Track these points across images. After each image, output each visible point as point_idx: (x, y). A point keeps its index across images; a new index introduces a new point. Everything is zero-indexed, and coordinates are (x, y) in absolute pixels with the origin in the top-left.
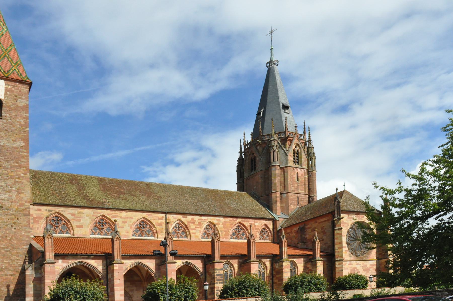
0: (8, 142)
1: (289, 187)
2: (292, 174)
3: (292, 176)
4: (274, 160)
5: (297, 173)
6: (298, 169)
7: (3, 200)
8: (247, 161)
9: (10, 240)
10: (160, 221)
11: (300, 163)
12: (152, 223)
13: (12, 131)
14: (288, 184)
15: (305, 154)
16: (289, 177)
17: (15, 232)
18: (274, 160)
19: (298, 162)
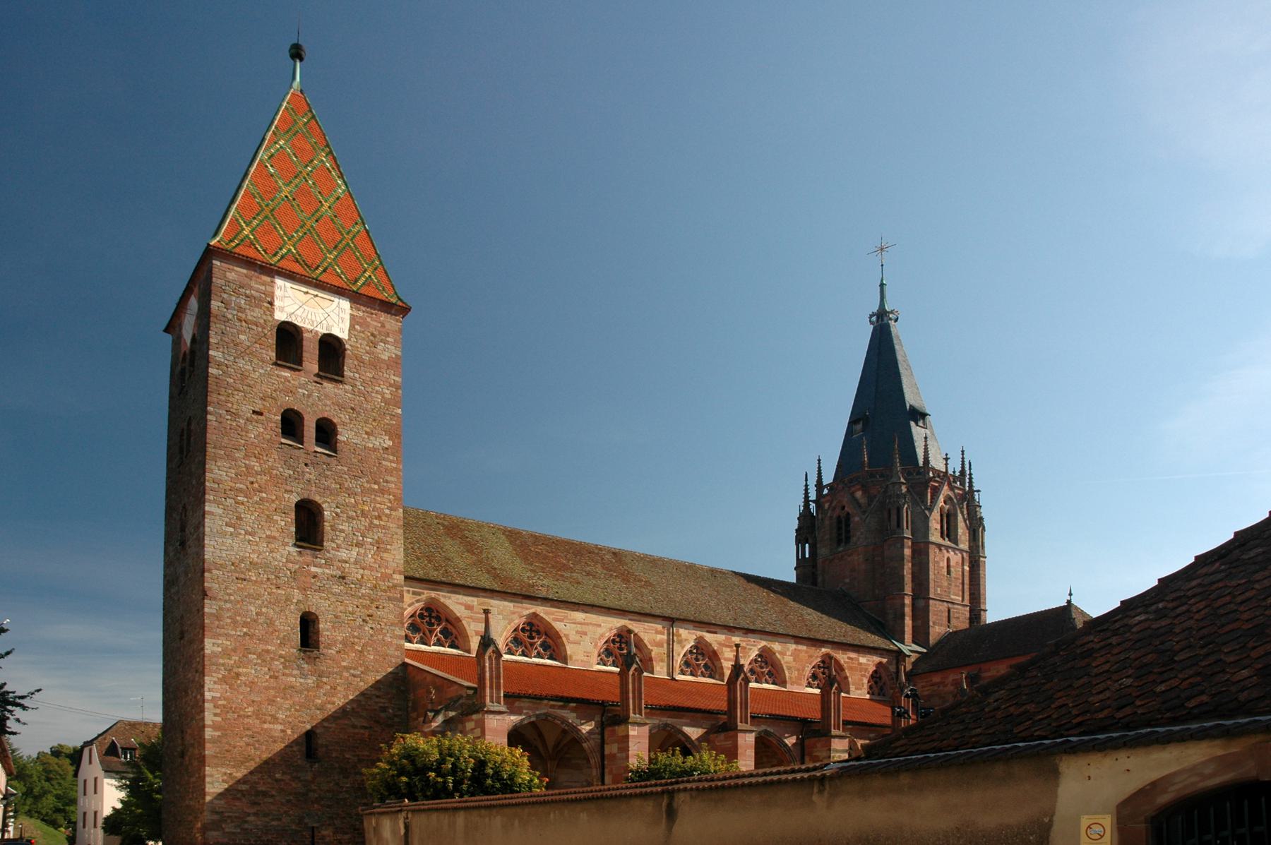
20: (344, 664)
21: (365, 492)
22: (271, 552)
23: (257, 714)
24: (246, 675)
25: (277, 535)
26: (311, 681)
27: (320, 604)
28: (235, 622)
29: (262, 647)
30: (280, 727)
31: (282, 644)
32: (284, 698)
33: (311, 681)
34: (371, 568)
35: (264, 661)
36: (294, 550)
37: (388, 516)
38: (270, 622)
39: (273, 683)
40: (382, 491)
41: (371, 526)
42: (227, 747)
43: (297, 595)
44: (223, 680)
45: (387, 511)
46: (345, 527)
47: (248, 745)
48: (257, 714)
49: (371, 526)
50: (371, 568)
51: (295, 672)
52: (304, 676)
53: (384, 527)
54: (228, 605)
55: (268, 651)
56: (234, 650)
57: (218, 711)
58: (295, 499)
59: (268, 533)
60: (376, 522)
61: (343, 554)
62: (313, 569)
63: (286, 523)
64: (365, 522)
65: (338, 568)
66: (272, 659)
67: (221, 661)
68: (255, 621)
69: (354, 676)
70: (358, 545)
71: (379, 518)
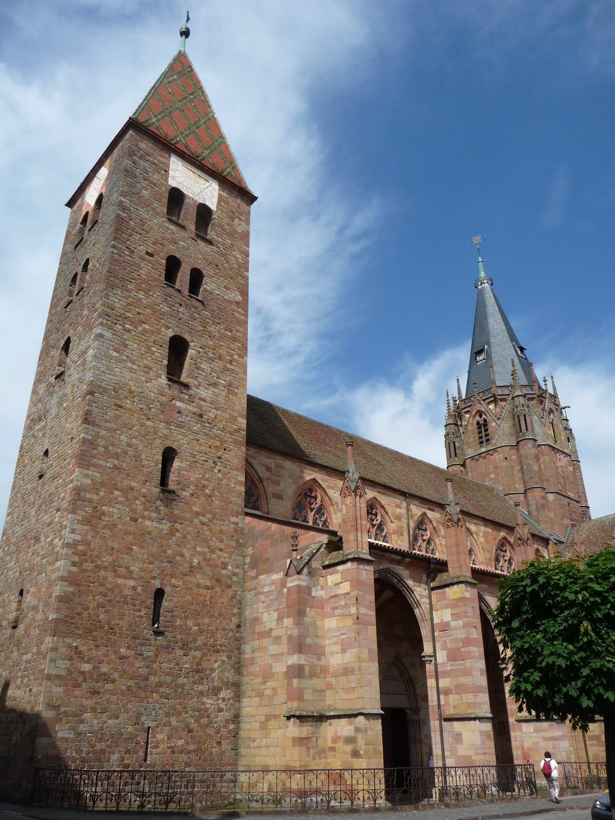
4: (527, 430)
8: (470, 428)
9: (210, 496)
10: (398, 510)
12: (387, 513)
17: (220, 480)
18: (527, 430)
20: (195, 509)
21: (222, 337)
22: (147, 382)
24: (111, 515)
25: (151, 365)
27: (180, 441)
29: (126, 483)
30: (131, 583)
33: (165, 527)
35: (128, 500)
36: (163, 380)
38: (137, 458)
41: (225, 369)
42: (79, 610)
44: (87, 521)
47: (100, 606)
48: (114, 567)
49: (225, 369)
51: (154, 515)
52: (159, 521)
53: (232, 371)
54: (103, 432)
55: (132, 488)
56: (103, 485)
57: (76, 559)
58: (170, 333)
59: (146, 362)
60: (228, 366)
63: (161, 355)
64: (218, 365)
65: (197, 406)
66: (137, 498)
67: (88, 496)
69: (203, 523)
70: (215, 385)
71: (231, 362)
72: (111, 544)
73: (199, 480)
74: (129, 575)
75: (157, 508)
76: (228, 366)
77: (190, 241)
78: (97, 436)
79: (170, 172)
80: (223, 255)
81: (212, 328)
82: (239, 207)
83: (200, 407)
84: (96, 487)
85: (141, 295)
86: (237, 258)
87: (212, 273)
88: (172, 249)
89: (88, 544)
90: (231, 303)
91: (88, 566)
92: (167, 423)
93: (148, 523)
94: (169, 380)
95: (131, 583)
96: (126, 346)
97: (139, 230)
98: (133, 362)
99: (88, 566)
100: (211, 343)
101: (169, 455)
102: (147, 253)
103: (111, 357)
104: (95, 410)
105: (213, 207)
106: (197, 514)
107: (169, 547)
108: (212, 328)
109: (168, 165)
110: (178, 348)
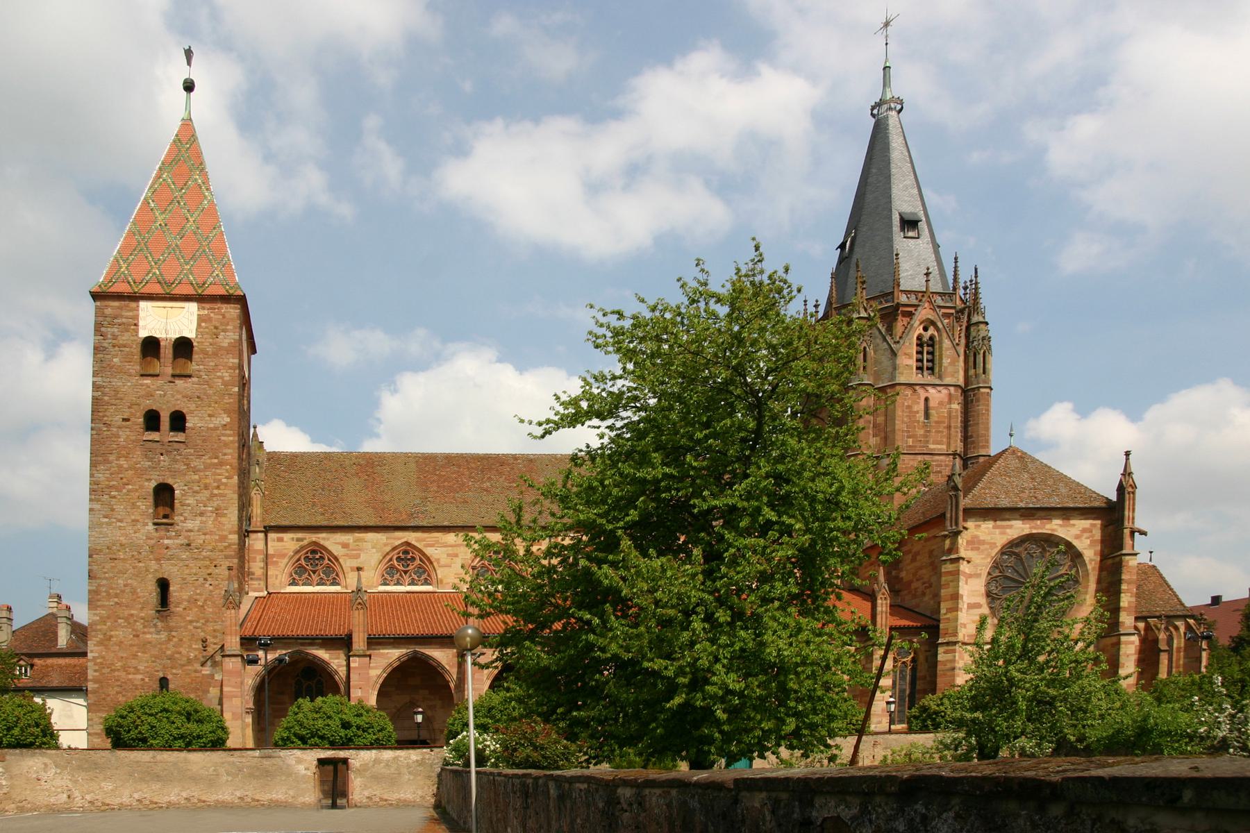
0: (202, 419)
1: (898, 436)
2: (908, 407)
3: (909, 407)
5: (927, 399)
6: (929, 388)
7: (191, 531)
11: (937, 370)
13: (208, 396)
14: (894, 431)
15: (956, 346)
16: (899, 413)
19: (931, 369)
21: (207, 467)
23: (125, 668)
24: (117, 636)
26: (163, 636)
28: (108, 594)
29: (126, 613)
31: (142, 609)
32: (144, 653)
33: (163, 636)
34: (211, 533)
36: (151, 527)
37: (226, 484)
38: (134, 592)
39: (136, 641)
40: (221, 464)
41: (213, 495)
43: (153, 565)
44: (100, 643)
45: (224, 480)
46: (191, 501)
48: (125, 668)
50: (211, 533)
51: (152, 630)
52: (158, 632)
54: (104, 582)
55: (132, 615)
56: (108, 618)
58: (153, 484)
60: (216, 492)
61: (189, 525)
62: (166, 542)
63: (146, 506)
64: (207, 493)
68: (123, 591)
70: (202, 514)
71: (218, 487)
72: (121, 654)
73: (190, 597)
74: (137, 671)
75: (155, 625)
76: (216, 492)
77: (167, 387)
78: (99, 585)
79: (141, 323)
80: (207, 383)
81: (196, 463)
82: (224, 317)
83: (188, 537)
84: (103, 621)
85: (122, 462)
86: (222, 378)
87: (193, 407)
88: (149, 404)
89: (103, 657)
90: (216, 429)
91: (106, 671)
92: (158, 560)
93: (148, 636)
94: (155, 524)
95: (140, 677)
96: (113, 510)
97: (113, 401)
98: (121, 521)
99: (106, 671)
100: (197, 477)
101: (163, 585)
102: (124, 420)
103: (102, 523)
104: (95, 567)
105: (190, 333)
106: (191, 622)
107: (167, 649)
108: (196, 463)
109: (137, 317)
110: (164, 495)
